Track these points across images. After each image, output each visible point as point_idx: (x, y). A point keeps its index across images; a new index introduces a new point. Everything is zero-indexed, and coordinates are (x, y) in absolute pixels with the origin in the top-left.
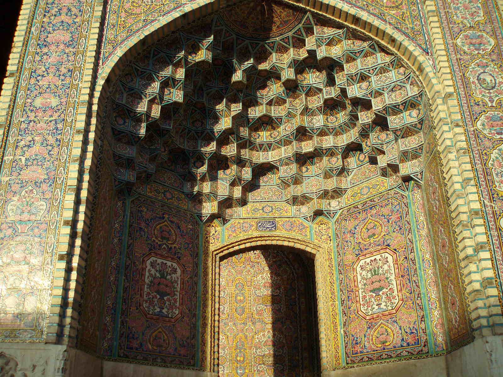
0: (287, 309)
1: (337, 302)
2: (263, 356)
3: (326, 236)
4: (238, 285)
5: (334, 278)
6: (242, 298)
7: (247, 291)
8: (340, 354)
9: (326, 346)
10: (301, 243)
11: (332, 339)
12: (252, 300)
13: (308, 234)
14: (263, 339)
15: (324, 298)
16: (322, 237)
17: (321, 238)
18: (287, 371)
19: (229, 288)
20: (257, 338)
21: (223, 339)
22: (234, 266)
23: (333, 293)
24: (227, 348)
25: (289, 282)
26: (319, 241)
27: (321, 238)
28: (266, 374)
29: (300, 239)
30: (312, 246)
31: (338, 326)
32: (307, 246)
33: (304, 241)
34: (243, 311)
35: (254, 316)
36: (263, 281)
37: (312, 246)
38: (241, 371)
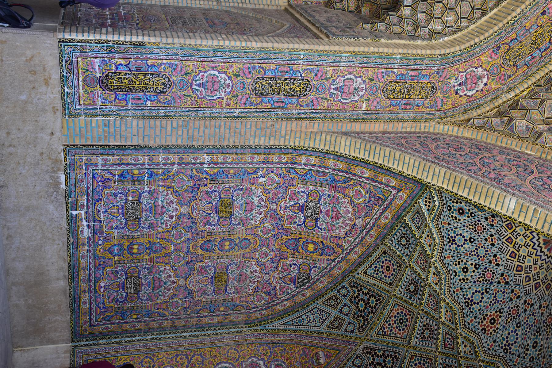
4: (247, 241)
12: (222, 260)
18: (116, 306)
19: (244, 230)
20: (165, 269)
24: (152, 232)
28: (112, 282)
36: (249, 273)
38: (116, 251)
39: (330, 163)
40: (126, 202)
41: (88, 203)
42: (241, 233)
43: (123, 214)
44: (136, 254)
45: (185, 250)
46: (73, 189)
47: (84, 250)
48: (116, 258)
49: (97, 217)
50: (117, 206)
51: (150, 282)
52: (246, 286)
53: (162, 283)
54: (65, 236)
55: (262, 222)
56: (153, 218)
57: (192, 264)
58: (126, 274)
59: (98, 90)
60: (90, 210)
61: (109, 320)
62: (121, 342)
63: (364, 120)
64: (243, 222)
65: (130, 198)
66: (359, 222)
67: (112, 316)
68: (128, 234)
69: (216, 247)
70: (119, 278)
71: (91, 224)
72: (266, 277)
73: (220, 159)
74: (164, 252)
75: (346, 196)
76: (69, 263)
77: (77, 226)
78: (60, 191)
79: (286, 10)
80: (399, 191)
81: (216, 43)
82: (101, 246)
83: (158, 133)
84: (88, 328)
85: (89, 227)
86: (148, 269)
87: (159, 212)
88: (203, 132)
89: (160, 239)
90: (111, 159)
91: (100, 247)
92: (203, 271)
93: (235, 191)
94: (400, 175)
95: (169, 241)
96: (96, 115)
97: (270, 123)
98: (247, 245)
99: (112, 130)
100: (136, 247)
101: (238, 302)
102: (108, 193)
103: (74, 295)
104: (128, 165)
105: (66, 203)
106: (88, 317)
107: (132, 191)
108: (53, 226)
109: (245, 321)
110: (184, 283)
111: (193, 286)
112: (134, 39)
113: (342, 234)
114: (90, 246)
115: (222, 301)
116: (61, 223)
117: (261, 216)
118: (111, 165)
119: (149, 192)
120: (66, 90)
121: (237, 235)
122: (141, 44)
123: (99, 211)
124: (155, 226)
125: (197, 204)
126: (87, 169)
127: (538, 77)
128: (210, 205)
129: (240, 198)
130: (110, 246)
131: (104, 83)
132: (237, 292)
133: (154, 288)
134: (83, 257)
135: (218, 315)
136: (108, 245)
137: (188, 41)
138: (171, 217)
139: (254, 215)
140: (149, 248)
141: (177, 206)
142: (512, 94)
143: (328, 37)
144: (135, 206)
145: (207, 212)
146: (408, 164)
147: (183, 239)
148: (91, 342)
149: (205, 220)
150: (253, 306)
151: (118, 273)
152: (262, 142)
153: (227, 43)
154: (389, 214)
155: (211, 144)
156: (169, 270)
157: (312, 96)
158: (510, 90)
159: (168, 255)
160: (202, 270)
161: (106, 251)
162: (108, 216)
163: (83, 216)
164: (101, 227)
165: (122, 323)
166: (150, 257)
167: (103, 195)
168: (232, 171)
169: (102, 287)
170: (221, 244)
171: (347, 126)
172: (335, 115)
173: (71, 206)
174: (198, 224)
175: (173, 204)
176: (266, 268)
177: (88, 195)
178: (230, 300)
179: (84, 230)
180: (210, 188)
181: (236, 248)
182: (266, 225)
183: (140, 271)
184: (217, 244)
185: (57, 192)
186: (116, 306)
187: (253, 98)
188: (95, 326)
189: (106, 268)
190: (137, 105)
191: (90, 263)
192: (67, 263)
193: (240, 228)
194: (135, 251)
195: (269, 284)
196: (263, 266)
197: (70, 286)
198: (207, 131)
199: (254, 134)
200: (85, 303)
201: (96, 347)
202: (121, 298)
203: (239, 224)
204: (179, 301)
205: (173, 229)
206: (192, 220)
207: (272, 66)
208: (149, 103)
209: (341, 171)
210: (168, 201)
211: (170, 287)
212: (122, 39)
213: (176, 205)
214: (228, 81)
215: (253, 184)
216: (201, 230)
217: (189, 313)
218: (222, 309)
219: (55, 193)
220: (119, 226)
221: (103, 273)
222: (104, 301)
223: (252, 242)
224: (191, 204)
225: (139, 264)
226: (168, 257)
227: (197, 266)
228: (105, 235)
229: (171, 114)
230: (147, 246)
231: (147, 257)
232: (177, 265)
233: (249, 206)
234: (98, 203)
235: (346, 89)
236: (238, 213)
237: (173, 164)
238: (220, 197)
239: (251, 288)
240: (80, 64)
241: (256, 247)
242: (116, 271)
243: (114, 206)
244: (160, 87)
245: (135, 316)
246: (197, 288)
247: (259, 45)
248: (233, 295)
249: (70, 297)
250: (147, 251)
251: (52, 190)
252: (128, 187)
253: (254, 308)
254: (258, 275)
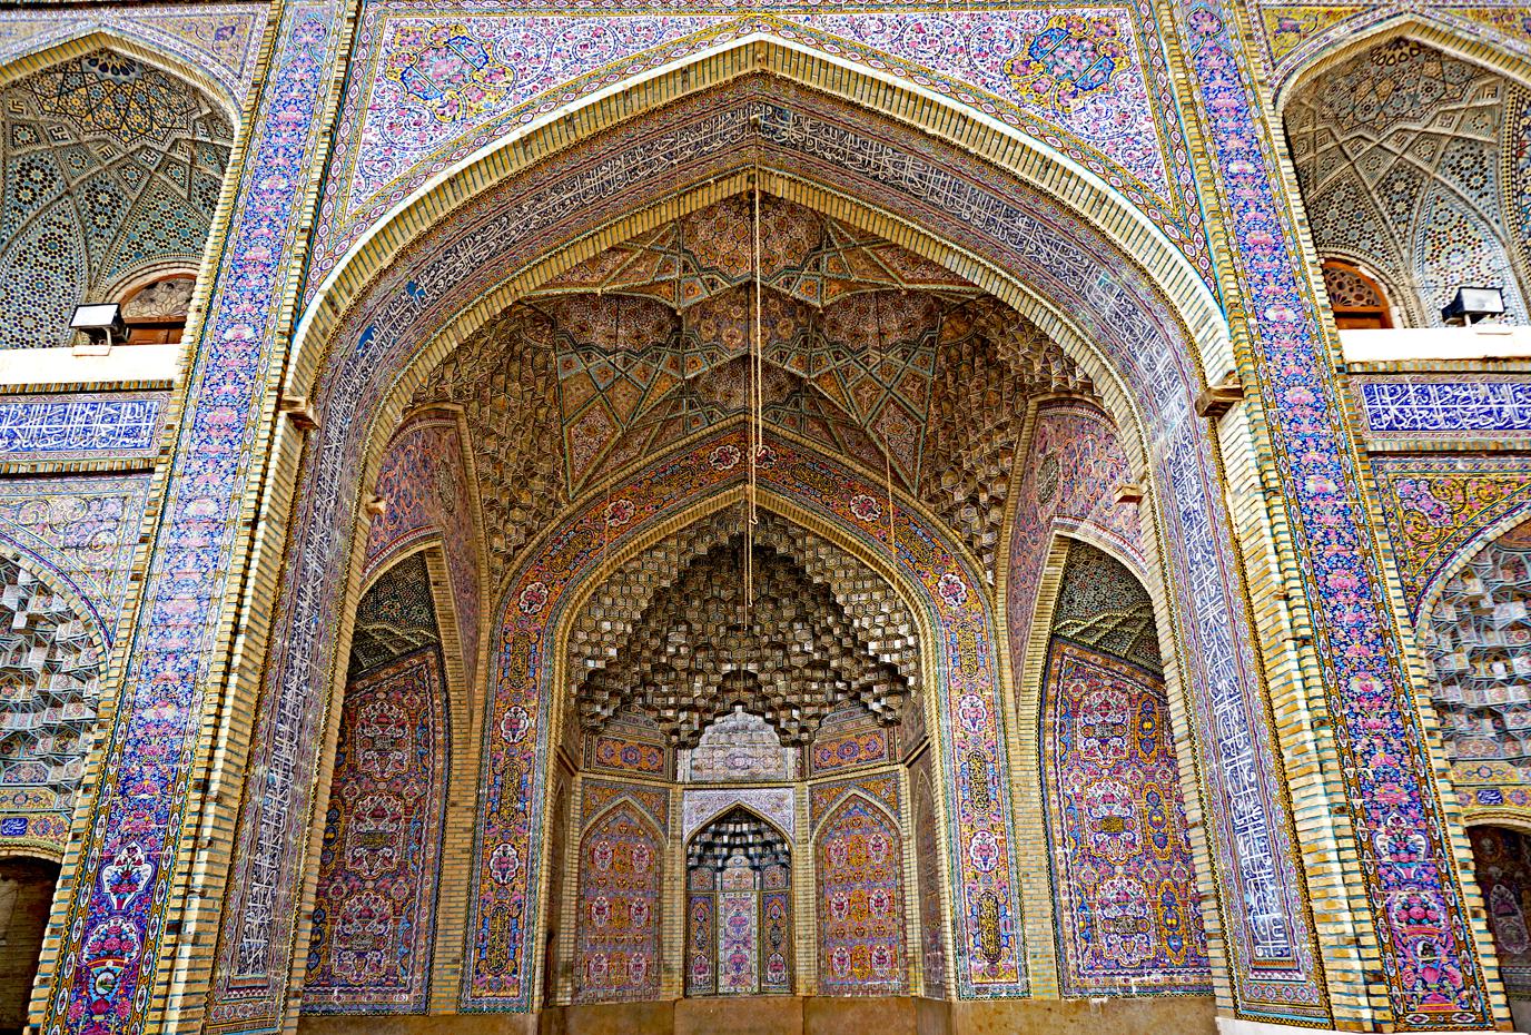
39: (1049, 721)
42: (1141, 804)
47: (1179, 979)
48: (1185, 943)
55: (1125, 783)
59: (1000, 963)
63: (1002, 691)
64: (1127, 803)
65: (1112, 929)
66: (1108, 682)
71: (1146, 971)
73: (1058, 837)
74: (1172, 889)
75: (1081, 701)
79: (909, 766)
80: (1064, 654)
81: (944, 851)
83: (1037, 903)
85: (1149, 974)
88: (1032, 857)
90: (1071, 950)
94: (1048, 659)
96: (1026, 966)
97: (1015, 789)
99: (1039, 950)
100: (1169, 921)
104: (1074, 933)
112: (949, 929)
113: (1126, 696)
114: (1172, 973)
118: (1077, 949)
120: (1004, 994)
122: (954, 923)
126: (1084, 975)
127: (941, 525)
131: (993, 958)
136: (1169, 952)
137: (946, 878)
138: (1130, 884)
140: (1170, 907)
142: (960, 544)
143: (926, 738)
146: (1036, 654)
152: (1036, 794)
153: (943, 840)
154: (1092, 658)
155: (1043, 847)
157: (983, 748)
158: (956, 548)
159: (1176, 884)
163: (1138, 979)
168: (1071, 822)
170: (1158, 824)
171: (1010, 707)
172: (1000, 722)
187: (993, 808)
190: (1012, 925)
194: (1174, 922)
198: (1030, 852)
199: (1029, 803)
207: (960, 793)
208: (1009, 913)
209: (1056, 710)
212: (950, 941)
214: (979, 835)
229: (1017, 890)
233: (1108, 799)
235: (973, 715)
236: (1117, 810)
237: (1069, 886)
240: (979, 980)
244: (991, 903)
247: (941, 808)
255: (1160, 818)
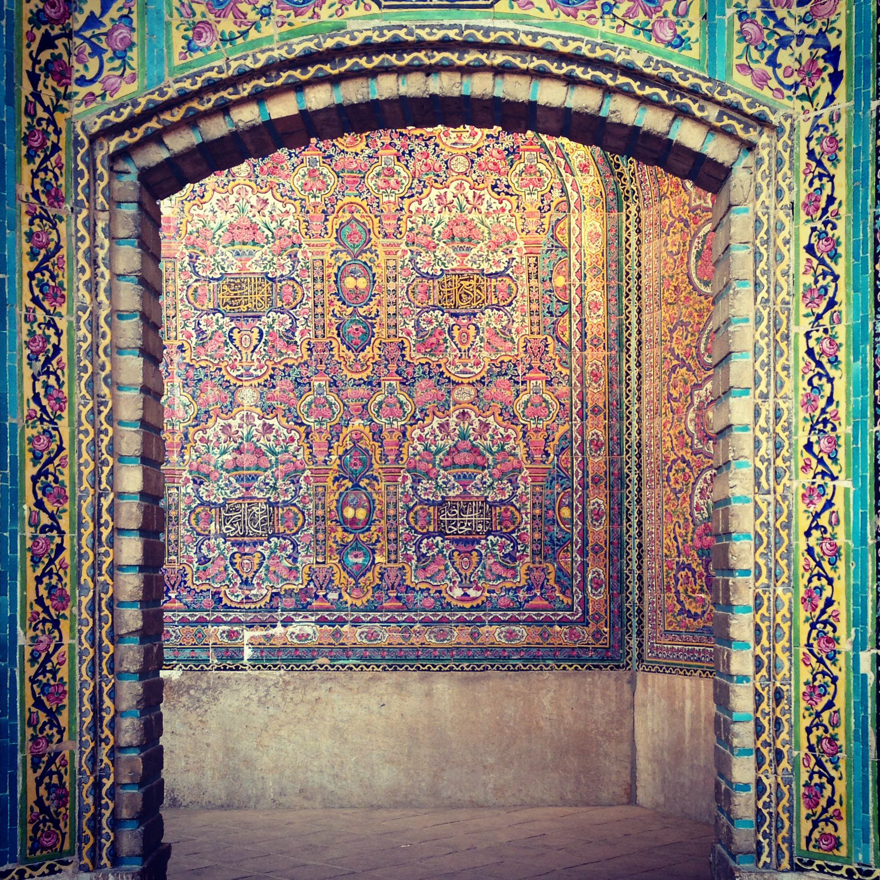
0: (535, 329)
1: (843, 483)
2: (440, 504)
3: (804, 50)
4: (347, 230)
5: (841, 332)
6: (362, 283)
7: (382, 257)
8: (841, 787)
9: (759, 730)
10: (648, 91)
11: (796, 690)
12: (401, 293)
13: (694, 33)
14: (440, 443)
15: (767, 448)
16: (784, 57)
17: (772, 62)
18: (528, 559)
19: (313, 241)
20: (420, 439)
21: (292, 439)
22: (331, 151)
23: (822, 424)
24: (307, 473)
25: (546, 221)
26: (762, 80)
27: (772, 62)
28: (452, 570)
29: (640, 63)
30: (711, 113)
31: (842, 627)
32: (682, 113)
33: (666, 83)
34: (368, 335)
35: (406, 352)
36: (446, 216)
37: (711, 113)
38: (360, 560)
40: (225, 536)
41: (225, 623)
42: (321, 250)
43: (255, 544)
44: (370, 511)
45: (363, 390)
46: (187, 653)
47: (352, 635)
49: (262, 604)
50: (233, 556)
51: (457, 477)
52: (488, 222)
53: (462, 445)
54: (307, 675)
55: (287, 197)
56: (269, 472)
57: (410, 370)
58: (428, 535)
60: (242, 619)
61: (572, 577)
62: (640, 545)
64: (290, 247)
67: (560, 569)
68: (312, 531)
69: (361, 311)
70: (440, 552)
71: (279, 616)
72: (460, 164)
74: (367, 442)
76: (384, 669)
77: (284, 648)
78: (188, 682)
82: (344, 594)
84: (592, 628)
85: (287, 622)
86: (417, 481)
87: (254, 458)
89: (330, 454)
91: (346, 597)
92: (434, 340)
93: (197, 274)
95: (336, 433)
98: (359, 228)
100: (349, 513)
101: (543, 238)
102: (198, 578)
103: (479, 660)
105: (218, 669)
106: (557, 628)
107: (193, 522)
108: (280, 700)
109: (609, 210)
110: (467, 388)
111: (477, 364)
114: (342, 622)
115: (533, 282)
116: (270, 683)
117: (271, 200)
119: (198, 482)
121: (327, 257)
123: (247, 598)
124: (292, 469)
125: (233, 368)
128: (236, 335)
129: (219, 259)
130: (344, 574)
132: (508, 242)
133: (476, 466)
134: (372, 636)
135: (581, 289)
136: (340, 577)
138: (268, 428)
139: (267, 219)
141: (238, 416)
144: (235, 515)
145: (255, 342)
147: (331, 398)
148: (635, 620)
149: (280, 344)
150: (556, 193)
151: (424, 555)
156: (422, 429)
159: (377, 434)
160: (430, 344)
161: (357, 583)
162: (259, 577)
163: (259, 633)
164: (289, 593)
165: (585, 543)
166: (381, 476)
167: (204, 588)
169: (465, 594)
173: (232, 658)
174: (290, 362)
175: (230, 426)
176: (430, 168)
177: (202, 622)
178: (532, 260)
179: (297, 632)
180: (189, 337)
181: (365, 257)
182: (297, 184)
183: (421, 502)
184: (350, 310)
185: (190, 687)
186: (528, 559)
188: (585, 611)
189: (408, 583)
191: (392, 620)
192: (384, 674)
193: (306, 253)
195: (479, 155)
196: (425, 178)
197: (451, 669)
200: (511, 635)
201: (646, 611)
202: (502, 547)
203: (293, 256)
204: (525, 398)
205: (302, 424)
206: (278, 378)
210: (223, 437)
211: (476, 425)
213: (233, 418)
215: (178, 230)
216: (306, 355)
217: (565, 372)
218: (560, 281)
219: (192, 692)
220: (290, 550)
221: (422, 591)
222: (509, 590)
223: (348, 216)
224: (233, 381)
225: (401, 504)
226: (385, 434)
227: (415, 356)
228: (312, 585)
230: (350, 484)
231: (382, 485)
232: (409, 409)
234: (225, 601)
238: (216, 311)
239: (496, 205)
241: (364, 204)
242: (418, 560)
243: (233, 564)
245: (566, 512)
246: (485, 354)
248: (515, 254)
249: (485, 669)
250: (362, 484)
251: (184, 699)
252: (183, 532)
253: (564, 191)
254: (452, 188)
255: (362, 283)
